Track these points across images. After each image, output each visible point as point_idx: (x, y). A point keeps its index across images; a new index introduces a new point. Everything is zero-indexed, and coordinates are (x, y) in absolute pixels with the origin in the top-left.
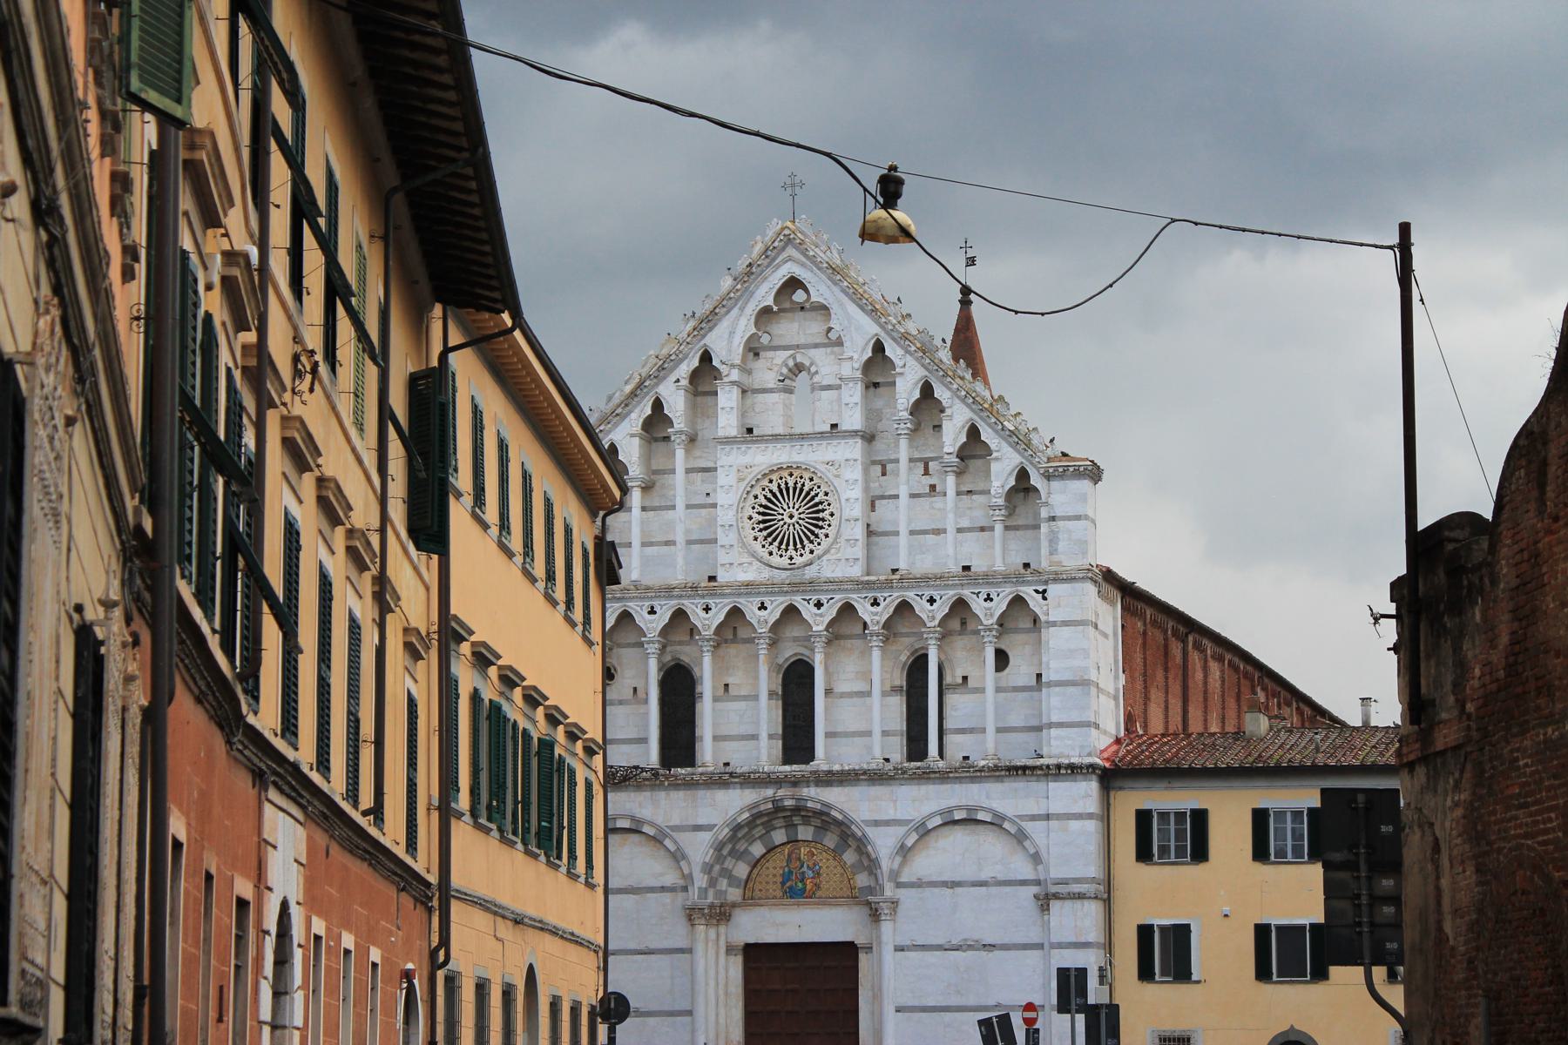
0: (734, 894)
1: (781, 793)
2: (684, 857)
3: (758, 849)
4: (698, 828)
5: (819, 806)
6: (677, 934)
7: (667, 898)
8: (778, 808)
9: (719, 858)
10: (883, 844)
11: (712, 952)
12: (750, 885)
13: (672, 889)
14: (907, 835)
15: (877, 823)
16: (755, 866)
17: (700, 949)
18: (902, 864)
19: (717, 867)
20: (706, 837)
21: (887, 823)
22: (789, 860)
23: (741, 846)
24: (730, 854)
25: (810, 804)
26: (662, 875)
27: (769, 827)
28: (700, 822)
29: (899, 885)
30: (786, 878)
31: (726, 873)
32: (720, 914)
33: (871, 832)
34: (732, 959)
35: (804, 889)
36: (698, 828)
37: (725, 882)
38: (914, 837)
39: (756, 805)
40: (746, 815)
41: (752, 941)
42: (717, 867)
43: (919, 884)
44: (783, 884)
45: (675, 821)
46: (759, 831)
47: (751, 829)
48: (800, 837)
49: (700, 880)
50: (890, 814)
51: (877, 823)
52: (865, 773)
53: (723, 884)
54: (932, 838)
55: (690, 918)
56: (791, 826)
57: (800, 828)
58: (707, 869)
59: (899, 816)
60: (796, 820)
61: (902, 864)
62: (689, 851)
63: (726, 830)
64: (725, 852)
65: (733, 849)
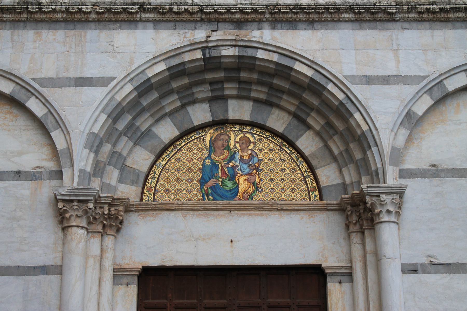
0: (129, 192)
1: (217, 36)
2: (60, 124)
3: (166, 131)
4: (83, 82)
5: (275, 58)
6: (38, 241)
7: (24, 188)
8: (211, 63)
9: (111, 134)
10: (381, 110)
11: (93, 274)
12: (151, 183)
13: (33, 176)
14: (416, 97)
15: (369, 80)
16: (159, 156)
17: (75, 264)
18: (409, 140)
19: (107, 148)
20: (98, 94)
21: (385, 80)
22: (212, 148)
23: (144, 123)
24: (125, 133)
25: (261, 54)
26: (20, 154)
27: (189, 100)
28: (88, 74)
29: (403, 174)
30: (208, 173)
31: (117, 159)
32: (108, 217)
33: (360, 91)
34: (122, 290)
35: (234, 192)
36: (83, 82)
37: (116, 173)
38: (426, 102)
39: (178, 52)
40: (162, 67)
41: (154, 262)
42: (107, 148)
43: (435, 172)
44: (202, 182)
45: (49, 70)
46: (172, 103)
47: (163, 97)
48: (232, 115)
49: (83, 160)
50: (390, 69)
51: (369, 80)
52: (351, 9)
53: (113, 175)
54: (450, 107)
55: (62, 220)
56: (218, 99)
57: (232, 103)
58: (95, 144)
59: (404, 71)
60: (230, 89)
61: (409, 140)
62: (69, 116)
63: (129, 88)
64: (121, 126)
65: (131, 125)
